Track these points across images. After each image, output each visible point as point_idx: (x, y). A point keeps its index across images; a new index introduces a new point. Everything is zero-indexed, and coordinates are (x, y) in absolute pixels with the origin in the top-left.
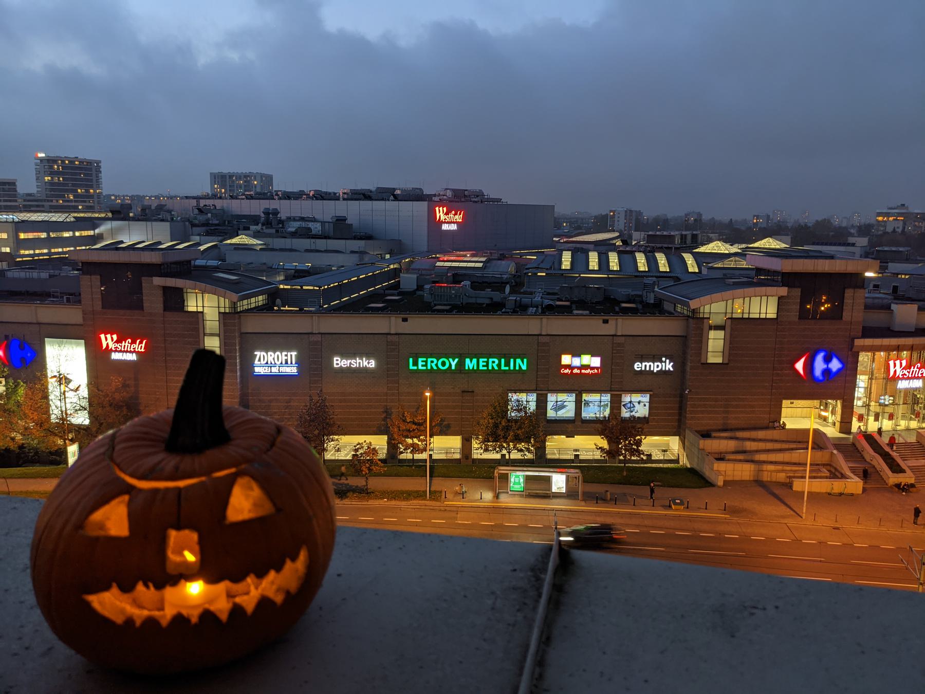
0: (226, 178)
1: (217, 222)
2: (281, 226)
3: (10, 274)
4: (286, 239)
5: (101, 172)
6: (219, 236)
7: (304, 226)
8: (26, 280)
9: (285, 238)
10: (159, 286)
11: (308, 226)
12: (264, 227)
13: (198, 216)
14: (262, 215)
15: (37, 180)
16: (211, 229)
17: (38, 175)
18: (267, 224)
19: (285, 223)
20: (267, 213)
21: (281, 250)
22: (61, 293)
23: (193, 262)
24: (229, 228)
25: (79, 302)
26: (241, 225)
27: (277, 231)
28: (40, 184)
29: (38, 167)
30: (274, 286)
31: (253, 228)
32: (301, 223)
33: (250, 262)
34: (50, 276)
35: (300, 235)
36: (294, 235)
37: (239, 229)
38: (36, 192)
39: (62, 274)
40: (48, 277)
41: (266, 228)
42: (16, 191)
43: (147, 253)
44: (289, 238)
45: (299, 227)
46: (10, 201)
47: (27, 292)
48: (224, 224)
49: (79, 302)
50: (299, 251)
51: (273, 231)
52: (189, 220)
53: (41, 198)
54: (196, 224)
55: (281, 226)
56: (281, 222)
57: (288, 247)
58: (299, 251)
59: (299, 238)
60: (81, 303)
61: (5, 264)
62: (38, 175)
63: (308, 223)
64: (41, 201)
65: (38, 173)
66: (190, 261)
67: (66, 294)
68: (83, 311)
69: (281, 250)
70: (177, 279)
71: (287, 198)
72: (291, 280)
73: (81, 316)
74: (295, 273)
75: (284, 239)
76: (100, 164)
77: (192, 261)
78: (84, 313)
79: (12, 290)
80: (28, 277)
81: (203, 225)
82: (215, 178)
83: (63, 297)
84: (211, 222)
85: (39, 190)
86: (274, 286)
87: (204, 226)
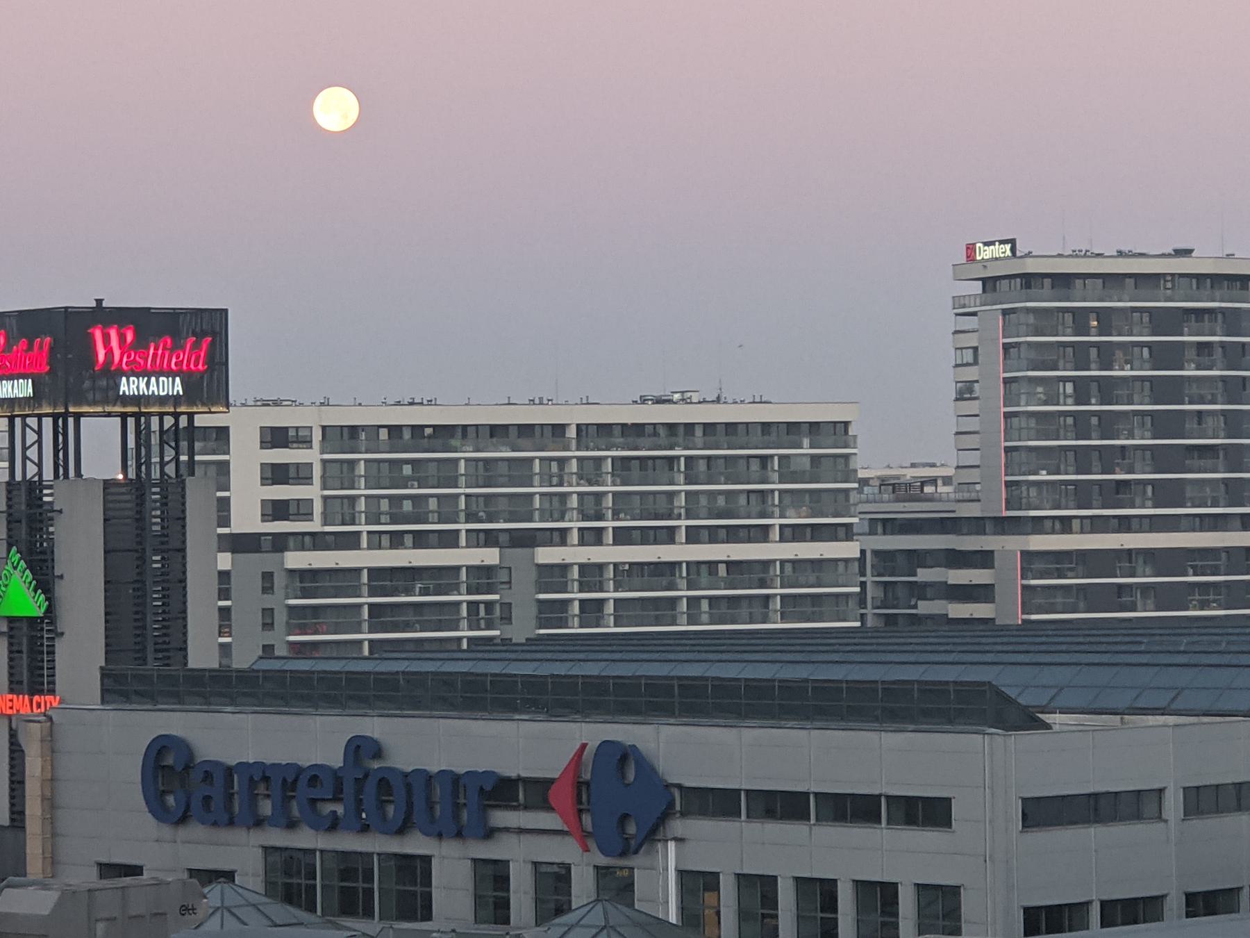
15: (960, 398)
17: (971, 373)
28: (973, 424)
29: (971, 323)
42: (846, 471)
53: (973, 511)
62: (971, 373)
64: (977, 525)
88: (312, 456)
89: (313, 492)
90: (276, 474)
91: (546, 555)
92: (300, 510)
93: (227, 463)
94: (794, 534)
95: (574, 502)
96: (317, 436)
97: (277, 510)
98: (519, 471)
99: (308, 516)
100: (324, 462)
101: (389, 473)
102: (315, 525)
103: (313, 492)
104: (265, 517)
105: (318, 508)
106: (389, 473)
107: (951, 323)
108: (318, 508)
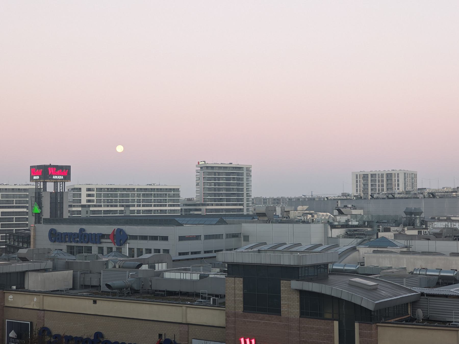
0: (368, 177)
1: (356, 223)
2: (424, 226)
3: (167, 275)
4: (429, 241)
5: (251, 176)
6: (359, 238)
7: (450, 227)
8: (181, 281)
9: (429, 239)
10: (296, 290)
11: (455, 227)
12: (406, 229)
13: (338, 218)
14: (404, 215)
15: (197, 185)
16: (350, 231)
17: (198, 181)
18: (409, 225)
19: (429, 224)
20: (409, 213)
21: (424, 253)
22: (208, 295)
23: (330, 267)
24: (369, 229)
25: (223, 304)
26: (381, 226)
27: (420, 232)
28: (198, 189)
29: (198, 174)
30: (415, 294)
31: (392, 229)
32: (447, 223)
33: (389, 266)
34: (202, 277)
35: (446, 237)
36: (438, 236)
37: (379, 230)
38: (195, 197)
39: (210, 276)
40: (198, 279)
41: (408, 229)
42: (179, 197)
43: (287, 255)
44: (433, 240)
45: (444, 228)
46: (174, 206)
47: (181, 292)
48: (363, 225)
49: (223, 304)
50: (443, 255)
51: (415, 232)
52: (328, 221)
53: (198, 203)
54: (335, 225)
55: (424, 226)
56: (423, 222)
57: (432, 249)
58: (443, 255)
59: (443, 240)
60: (224, 305)
61: (164, 265)
62: (198, 181)
63: (455, 224)
64: (199, 205)
65: (198, 179)
66: (328, 264)
67: (212, 295)
68: (226, 313)
69: (424, 253)
70: (314, 284)
71: (431, 196)
72: (434, 287)
73: (225, 318)
74: (439, 279)
75: (427, 241)
76: (250, 169)
77: (329, 264)
78: (227, 316)
79: (168, 290)
80: (182, 278)
81: (343, 226)
82: (357, 178)
83: (209, 299)
84: (350, 223)
85: (198, 194)
86: (415, 294)
87: (344, 228)
88: (94, 193)
89: (94, 198)
90: (89, 195)
91: (131, 208)
92: (93, 201)
93: (81, 193)
94: (170, 206)
95: (136, 200)
96: (95, 189)
97: (89, 201)
98: (128, 195)
99: (94, 202)
100: (96, 194)
101: (105, 196)
102: (95, 203)
103: (94, 198)
104: (87, 202)
105: (95, 201)
106: (105, 196)
107: (196, 174)
108: (95, 201)
